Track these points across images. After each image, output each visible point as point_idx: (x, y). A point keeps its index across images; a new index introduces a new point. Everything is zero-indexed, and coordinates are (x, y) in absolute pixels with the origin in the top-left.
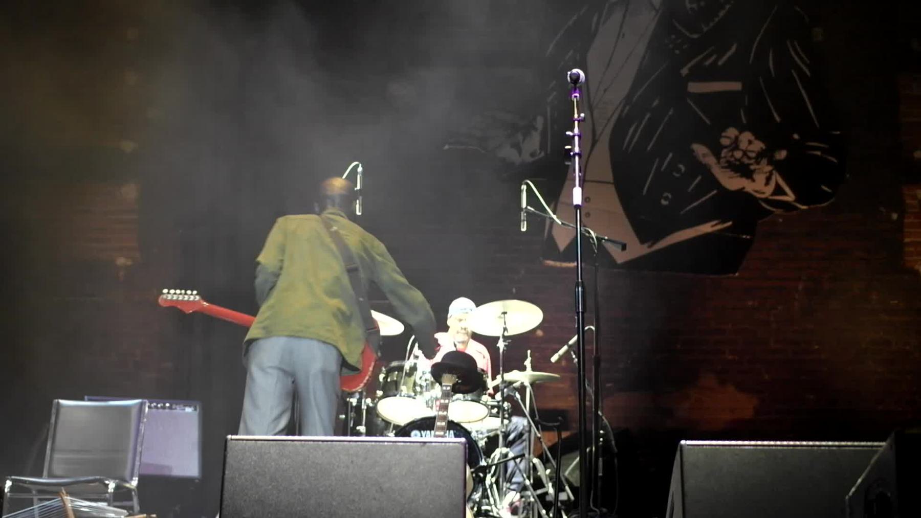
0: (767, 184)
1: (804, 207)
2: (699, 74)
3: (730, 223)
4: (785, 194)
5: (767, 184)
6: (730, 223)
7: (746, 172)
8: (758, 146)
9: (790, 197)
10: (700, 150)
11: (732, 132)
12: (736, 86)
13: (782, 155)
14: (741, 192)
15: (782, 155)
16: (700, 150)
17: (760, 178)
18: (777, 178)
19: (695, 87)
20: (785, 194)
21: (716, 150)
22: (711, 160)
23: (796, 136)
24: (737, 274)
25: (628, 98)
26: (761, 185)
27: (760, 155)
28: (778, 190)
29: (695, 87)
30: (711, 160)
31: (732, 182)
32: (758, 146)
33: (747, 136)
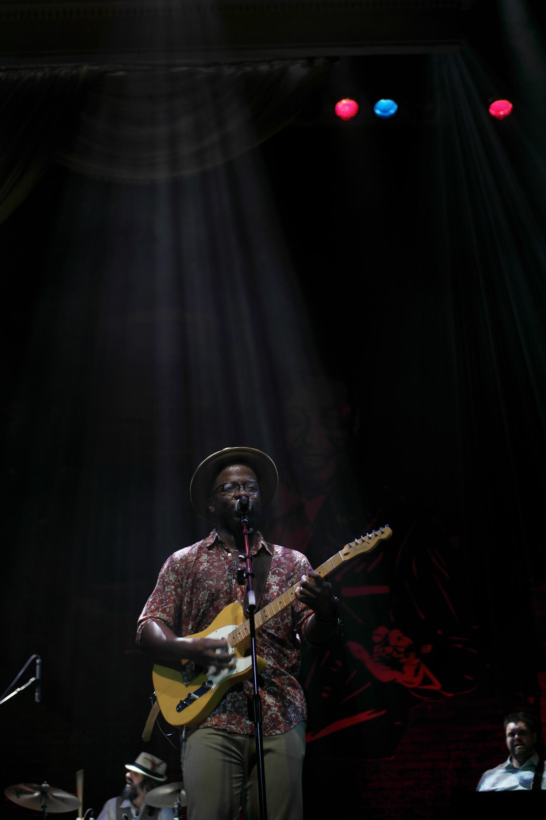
0: (416, 675)
1: (450, 695)
3: (384, 712)
4: (432, 683)
5: (416, 675)
6: (384, 712)
8: (407, 641)
9: (437, 686)
13: (428, 649)
15: (428, 649)
20: (432, 683)
23: (440, 632)
24: (393, 757)
28: (426, 681)
31: (385, 675)
32: (407, 641)
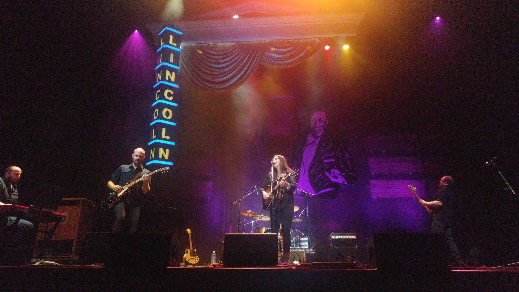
2: (326, 158)
7: (336, 177)
9: (346, 183)
10: (327, 173)
11: (333, 170)
12: (334, 160)
14: (336, 183)
16: (327, 173)
17: (339, 179)
18: (343, 179)
19: (325, 161)
21: (330, 173)
22: (329, 176)
25: (312, 163)
26: (340, 180)
27: (339, 174)
28: (344, 182)
29: (325, 161)
30: (329, 176)
31: (334, 180)
33: (337, 170)
